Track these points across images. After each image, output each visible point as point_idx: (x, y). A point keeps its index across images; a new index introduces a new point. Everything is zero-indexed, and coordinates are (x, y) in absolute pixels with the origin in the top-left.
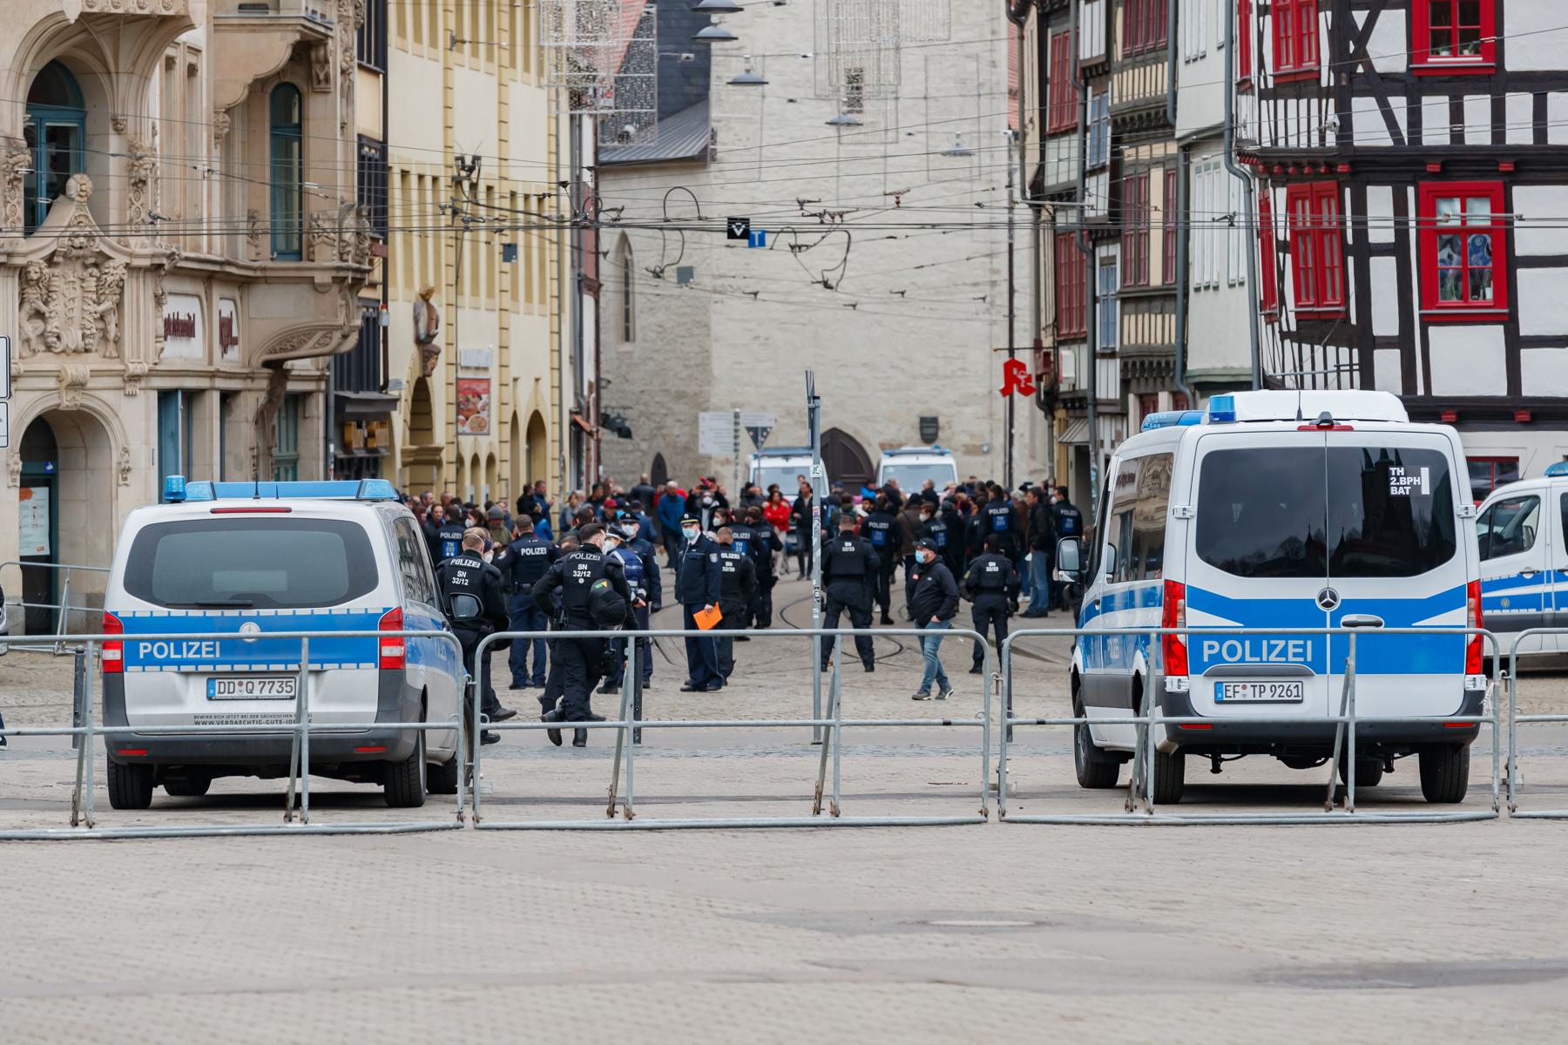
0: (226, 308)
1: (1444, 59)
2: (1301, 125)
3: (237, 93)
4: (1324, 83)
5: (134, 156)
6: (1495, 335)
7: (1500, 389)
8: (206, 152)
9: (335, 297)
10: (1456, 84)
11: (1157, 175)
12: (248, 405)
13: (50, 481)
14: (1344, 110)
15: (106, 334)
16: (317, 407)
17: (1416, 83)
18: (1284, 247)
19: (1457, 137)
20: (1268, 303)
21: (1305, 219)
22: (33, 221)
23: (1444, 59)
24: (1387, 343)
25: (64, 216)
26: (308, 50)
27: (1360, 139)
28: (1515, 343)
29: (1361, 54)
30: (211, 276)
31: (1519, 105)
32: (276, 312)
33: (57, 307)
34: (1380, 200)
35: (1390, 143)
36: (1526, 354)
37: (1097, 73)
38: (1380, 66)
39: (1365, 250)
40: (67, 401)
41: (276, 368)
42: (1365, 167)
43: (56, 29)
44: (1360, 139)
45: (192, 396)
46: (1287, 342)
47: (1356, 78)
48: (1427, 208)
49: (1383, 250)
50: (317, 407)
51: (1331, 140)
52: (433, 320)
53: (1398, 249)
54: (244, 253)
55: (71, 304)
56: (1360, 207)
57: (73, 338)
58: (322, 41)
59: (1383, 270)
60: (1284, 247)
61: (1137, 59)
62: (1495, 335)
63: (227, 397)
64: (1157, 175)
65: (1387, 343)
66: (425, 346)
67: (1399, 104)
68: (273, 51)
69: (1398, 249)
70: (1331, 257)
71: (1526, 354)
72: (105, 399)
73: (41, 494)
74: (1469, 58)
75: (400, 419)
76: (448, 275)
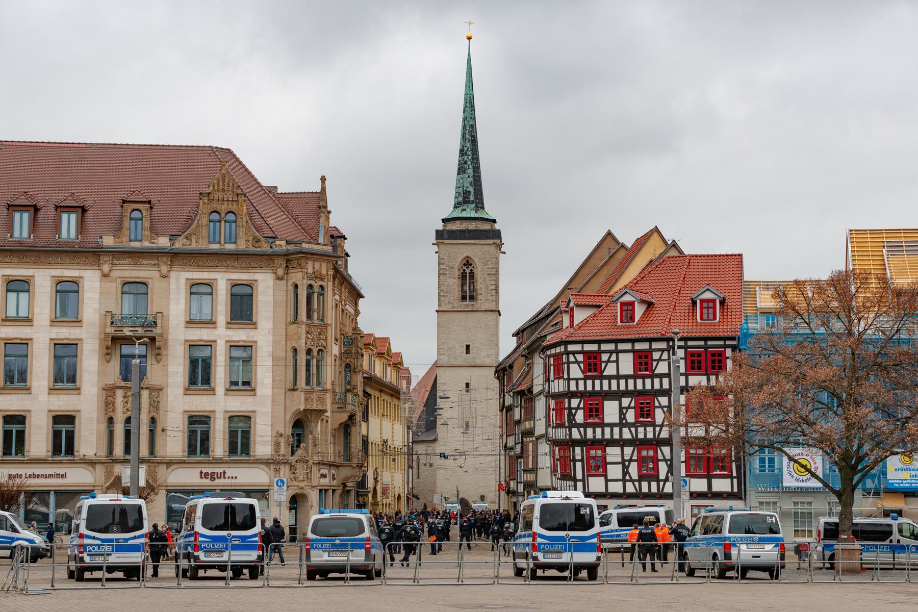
0: (334, 472)
1: (591, 420)
2: (561, 434)
3: (337, 426)
5: (314, 439)
6: (603, 478)
7: (604, 490)
8: (330, 438)
9: (356, 469)
10: (594, 426)
11: (531, 444)
12: (338, 493)
13: (296, 509)
15: (308, 477)
16: (353, 493)
17: (585, 425)
19: (594, 437)
20: (554, 472)
21: (562, 454)
22: (293, 453)
23: (591, 420)
24: (580, 480)
25: (299, 452)
26: (352, 417)
27: (574, 437)
28: (607, 481)
29: (574, 419)
30: (330, 465)
32: (344, 472)
33: (298, 471)
35: (579, 437)
36: (609, 483)
37: (518, 422)
39: (575, 461)
40: (299, 492)
41: (344, 485)
42: (575, 443)
43: (298, 412)
44: (574, 437)
45: (326, 490)
47: (573, 424)
48: (588, 452)
49: (579, 461)
50: (353, 493)
52: (378, 474)
53: (582, 460)
54: (338, 460)
55: (301, 471)
56: (574, 451)
57: (301, 478)
58: (355, 415)
59: (579, 465)
61: (527, 420)
62: (603, 478)
63: (334, 491)
64: (531, 444)
65: (580, 480)
66: (376, 480)
68: (344, 417)
69: (582, 460)
70: (568, 462)
71: (609, 483)
72: (308, 491)
73: (293, 511)
74: (597, 420)
75: (370, 495)
76: (381, 465)
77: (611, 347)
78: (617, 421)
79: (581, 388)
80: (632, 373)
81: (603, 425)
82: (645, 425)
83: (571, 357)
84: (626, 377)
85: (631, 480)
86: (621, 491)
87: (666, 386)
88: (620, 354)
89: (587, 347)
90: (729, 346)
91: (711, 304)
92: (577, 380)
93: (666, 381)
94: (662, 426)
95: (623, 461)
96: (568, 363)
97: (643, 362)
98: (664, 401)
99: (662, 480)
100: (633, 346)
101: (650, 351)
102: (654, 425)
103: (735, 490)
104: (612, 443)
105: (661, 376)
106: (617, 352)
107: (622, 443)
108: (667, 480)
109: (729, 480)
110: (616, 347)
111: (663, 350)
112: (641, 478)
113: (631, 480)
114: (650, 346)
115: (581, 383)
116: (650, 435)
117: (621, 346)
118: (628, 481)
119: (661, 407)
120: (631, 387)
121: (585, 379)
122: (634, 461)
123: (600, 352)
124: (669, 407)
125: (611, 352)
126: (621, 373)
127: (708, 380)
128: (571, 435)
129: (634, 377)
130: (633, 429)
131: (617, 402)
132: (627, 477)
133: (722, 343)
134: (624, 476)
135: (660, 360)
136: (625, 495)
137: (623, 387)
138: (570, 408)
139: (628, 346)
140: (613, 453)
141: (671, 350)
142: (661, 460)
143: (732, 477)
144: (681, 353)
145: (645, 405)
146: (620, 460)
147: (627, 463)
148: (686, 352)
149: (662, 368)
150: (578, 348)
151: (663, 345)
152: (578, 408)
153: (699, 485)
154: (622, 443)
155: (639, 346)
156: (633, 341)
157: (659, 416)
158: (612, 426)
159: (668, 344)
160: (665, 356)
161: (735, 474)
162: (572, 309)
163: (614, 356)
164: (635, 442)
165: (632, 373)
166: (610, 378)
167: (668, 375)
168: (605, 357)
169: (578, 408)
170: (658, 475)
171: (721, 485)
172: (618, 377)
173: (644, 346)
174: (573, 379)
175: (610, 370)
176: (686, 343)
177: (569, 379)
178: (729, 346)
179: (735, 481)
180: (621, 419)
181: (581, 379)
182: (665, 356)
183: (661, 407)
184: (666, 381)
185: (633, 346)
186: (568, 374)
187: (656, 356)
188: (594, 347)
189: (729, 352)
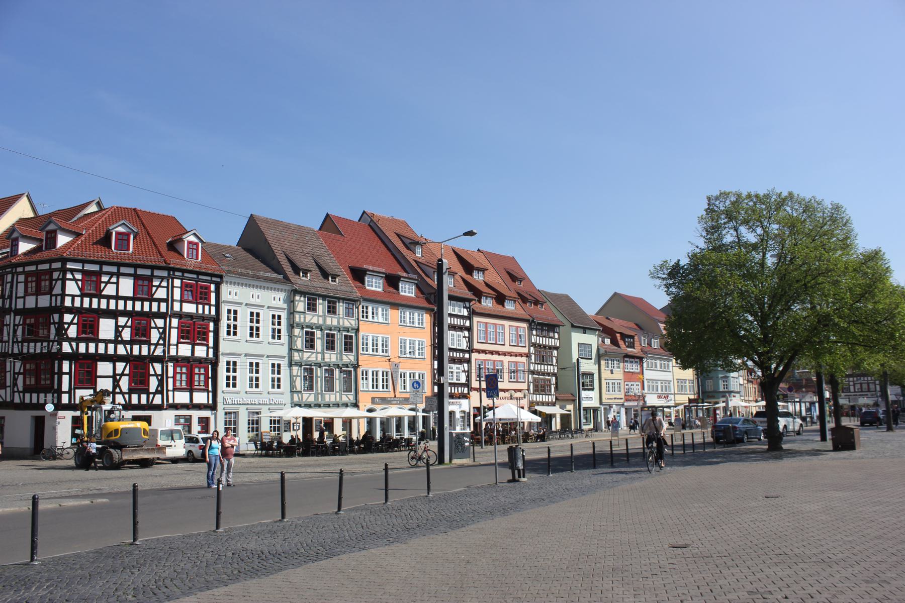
4: (52, 337)
18: (19, 373)
31: (102, 346)
38: (70, 336)
46: (16, 394)
53: (70, 373)
67: (74, 344)
69: (70, 373)
74: (91, 336)
77: (114, 269)
78: (112, 337)
79: (77, 303)
80: (131, 295)
81: (97, 341)
82: (140, 343)
83: (69, 276)
84: (126, 299)
85: (121, 393)
87: (163, 308)
89: (88, 267)
92: (73, 296)
93: (163, 306)
94: (157, 344)
95: (114, 376)
96: (64, 280)
98: (160, 322)
100: (135, 271)
101: (150, 279)
102: (149, 343)
103: (211, 402)
104: (106, 358)
105: (159, 301)
106: (119, 275)
107: (114, 359)
108: (157, 392)
109: (206, 394)
110: (119, 270)
112: (131, 391)
113: (121, 393)
114: (152, 273)
116: (145, 352)
117: (123, 270)
118: (118, 393)
119: (156, 327)
120: (129, 308)
121: (83, 296)
122: (126, 375)
123: (99, 274)
124: (164, 328)
126: (120, 294)
129: (134, 299)
132: (118, 390)
134: (114, 387)
139: (131, 271)
140: (104, 368)
146: (111, 374)
147: (118, 377)
148: (182, 283)
149: (161, 293)
150: (78, 266)
151: (165, 273)
152: (72, 323)
153: (182, 397)
155: (140, 272)
156: (136, 266)
157: (155, 336)
158: (106, 342)
159: (169, 274)
161: (210, 389)
163: (114, 280)
165: (131, 295)
166: (108, 298)
167: (166, 301)
169: (72, 323)
171: (201, 398)
172: (117, 298)
173: (148, 272)
175: (110, 290)
179: (210, 394)
180: (116, 336)
182: (164, 284)
183: (156, 327)
184: (163, 306)
188: (96, 268)
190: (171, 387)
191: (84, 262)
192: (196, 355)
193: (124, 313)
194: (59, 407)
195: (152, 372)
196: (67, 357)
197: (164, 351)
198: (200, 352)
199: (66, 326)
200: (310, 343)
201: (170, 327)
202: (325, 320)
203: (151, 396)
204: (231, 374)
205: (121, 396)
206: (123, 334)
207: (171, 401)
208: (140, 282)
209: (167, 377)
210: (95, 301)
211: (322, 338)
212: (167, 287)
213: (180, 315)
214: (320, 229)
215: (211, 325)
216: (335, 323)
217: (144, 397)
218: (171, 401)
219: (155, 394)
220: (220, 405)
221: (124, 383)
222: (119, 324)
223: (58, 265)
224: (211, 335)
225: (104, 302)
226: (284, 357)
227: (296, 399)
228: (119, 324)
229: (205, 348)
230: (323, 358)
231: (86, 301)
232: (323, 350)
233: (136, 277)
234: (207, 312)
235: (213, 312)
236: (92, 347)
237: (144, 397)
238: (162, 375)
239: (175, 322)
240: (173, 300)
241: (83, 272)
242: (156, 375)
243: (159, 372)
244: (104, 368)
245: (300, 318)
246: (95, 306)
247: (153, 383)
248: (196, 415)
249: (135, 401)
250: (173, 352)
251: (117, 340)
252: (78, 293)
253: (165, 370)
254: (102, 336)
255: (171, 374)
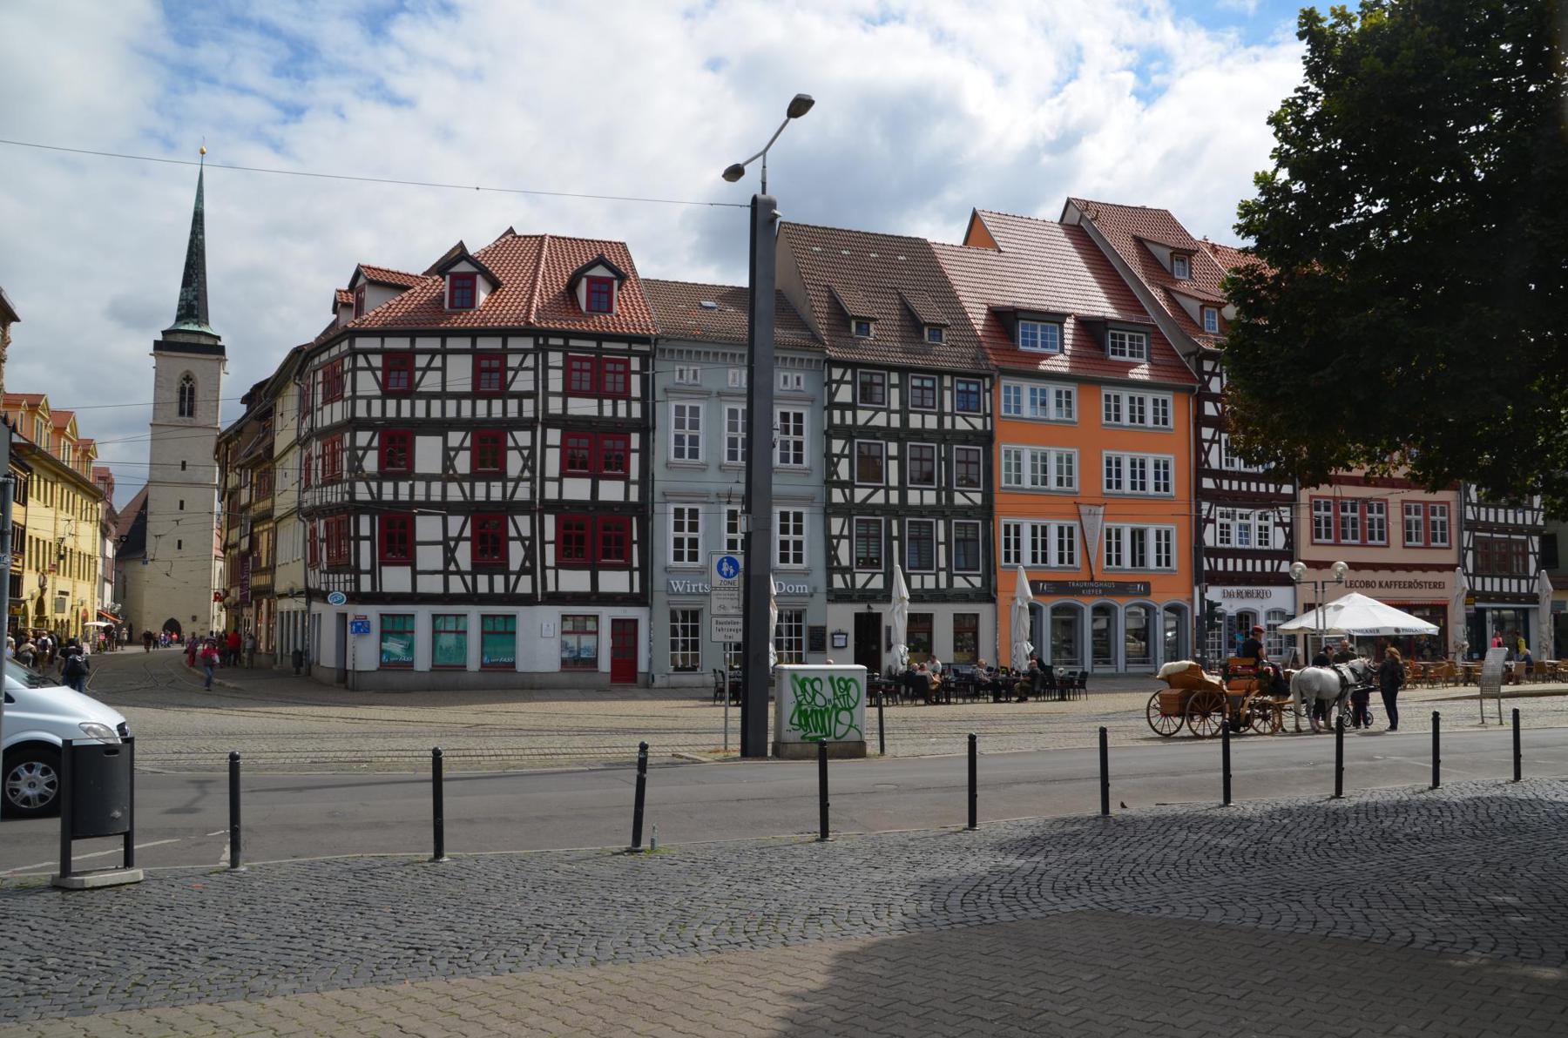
2: (334, 495)
6: (408, 569)
7: (409, 590)
14: (353, 487)
18: (322, 540)
24: (366, 572)
27: (359, 497)
28: (415, 573)
29: (360, 467)
34: (365, 521)
35: (368, 498)
39: (358, 538)
44: (359, 497)
47: (357, 472)
49: (365, 538)
51: (347, 497)
53: (371, 538)
59: (365, 546)
60: (322, 540)
62: (408, 569)
67: (374, 485)
69: (371, 538)
77: (435, 343)
78: (438, 470)
79: (376, 412)
80: (468, 388)
82: (488, 478)
83: (361, 362)
84: (459, 396)
85: (459, 572)
86: (439, 589)
88: (449, 358)
89: (393, 343)
90: (636, 354)
91: (605, 288)
92: (369, 399)
93: (528, 405)
94: (518, 480)
95: (445, 542)
96: (355, 370)
97: (490, 376)
98: (524, 438)
99: (513, 573)
100: (474, 343)
101: (502, 355)
103: (637, 589)
104: (428, 507)
105: (521, 396)
106: (445, 353)
107: (446, 508)
108: (523, 571)
109: (626, 574)
111: (525, 352)
112: (477, 569)
113: (459, 572)
115: (376, 404)
116: (496, 493)
117: (452, 343)
119: (518, 448)
120: (466, 412)
122: (466, 539)
123: (413, 352)
124: (532, 448)
125: (433, 353)
127: (600, 406)
128: (352, 493)
129: (474, 395)
130: (466, 486)
131: (440, 439)
132: (452, 567)
133: (624, 346)
134: (447, 562)
135: (521, 368)
136: (446, 598)
137: (451, 413)
138: (353, 447)
139: (465, 343)
141: (542, 350)
142: (514, 539)
143: (631, 570)
144: (556, 358)
145: (489, 444)
147: (452, 544)
149: (523, 382)
150: (374, 343)
151: (528, 343)
152: (367, 449)
153: (576, 580)
154: (446, 508)
155: (483, 343)
156: (473, 334)
157: (514, 463)
158: (428, 478)
159: (536, 343)
160: (530, 361)
161: (636, 564)
162: (362, 290)
163: (437, 362)
164: (466, 508)
165: (468, 388)
168: (421, 361)
169: (367, 449)
170: (507, 564)
171: (614, 581)
172: (443, 395)
173: (494, 343)
174: (362, 397)
175: (431, 382)
176: (566, 343)
177: (354, 398)
178: (636, 354)
179: (636, 575)
180: (445, 469)
181: (376, 397)
182: (530, 361)
183: (518, 448)
184: (528, 405)
185: (474, 343)
186: (354, 389)
187: (513, 361)
189: (635, 364)
190: (550, 559)
191: (382, 333)
192: (602, 497)
193: (457, 424)
194: (356, 597)
195: (512, 532)
196: (364, 508)
197: (533, 492)
198: (611, 491)
199: (360, 453)
200: (870, 470)
201: (544, 446)
202: (905, 421)
203: (513, 578)
204: (791, 537)
205: (458, 578)
206: (456, 463)
207: (551, 588)
208: (485, 364)
209: (543, 543)
210: (406, 404)
211: (901, 458)
212: (535, 369)
213: (566, 423)
214: (966, 243)
215: (635, 441)
216: (931, 422)
217: (499, 581)
218: (551, 588)
219: (519, 574)
220: (659, 598)
221: (464, 554)
222: (450, 444)
223: (345, 346)
224: (635, 459)
225: (421, 405)
226: (812, 499)
227: (838, 582)
228: (450, 444)
229: (621, 484)
230: (903, 496)
231: (391, 404)
232: (902, 481)
233: (478, 355)
234: (622, 413)
235: (636, 411)
236: (404, 487)
237: (499, 581)
238: (532, 538)
239: (554, 436)
240: (547, 394)
241: (387, 354)
242: (520, 538)
243: (526, 532)
244: (428, 528)
245: (843, 418)
246: (406, 413)
247: (516, 554)
248: (607, 614)
249: (483, 587)
250: (551, 492)
251: (448, 475)
252: (379, 393)
253: (538, 528)
254: (421, 467)
255: (550, 534)
